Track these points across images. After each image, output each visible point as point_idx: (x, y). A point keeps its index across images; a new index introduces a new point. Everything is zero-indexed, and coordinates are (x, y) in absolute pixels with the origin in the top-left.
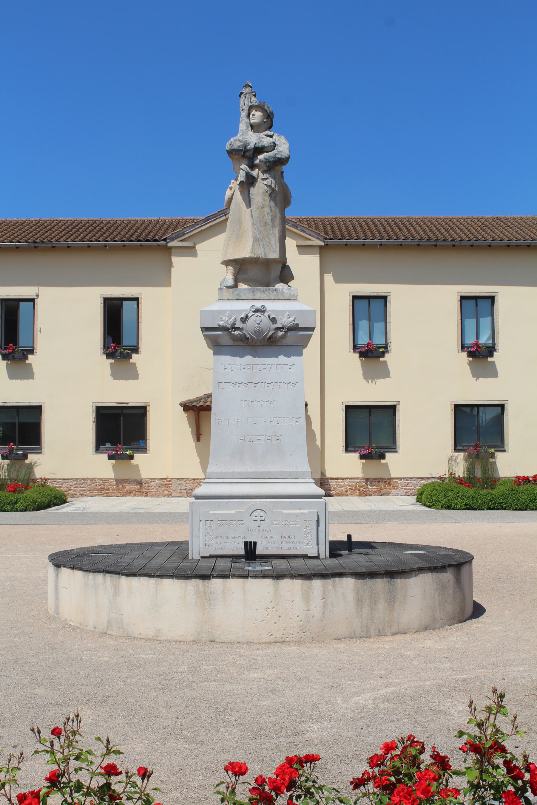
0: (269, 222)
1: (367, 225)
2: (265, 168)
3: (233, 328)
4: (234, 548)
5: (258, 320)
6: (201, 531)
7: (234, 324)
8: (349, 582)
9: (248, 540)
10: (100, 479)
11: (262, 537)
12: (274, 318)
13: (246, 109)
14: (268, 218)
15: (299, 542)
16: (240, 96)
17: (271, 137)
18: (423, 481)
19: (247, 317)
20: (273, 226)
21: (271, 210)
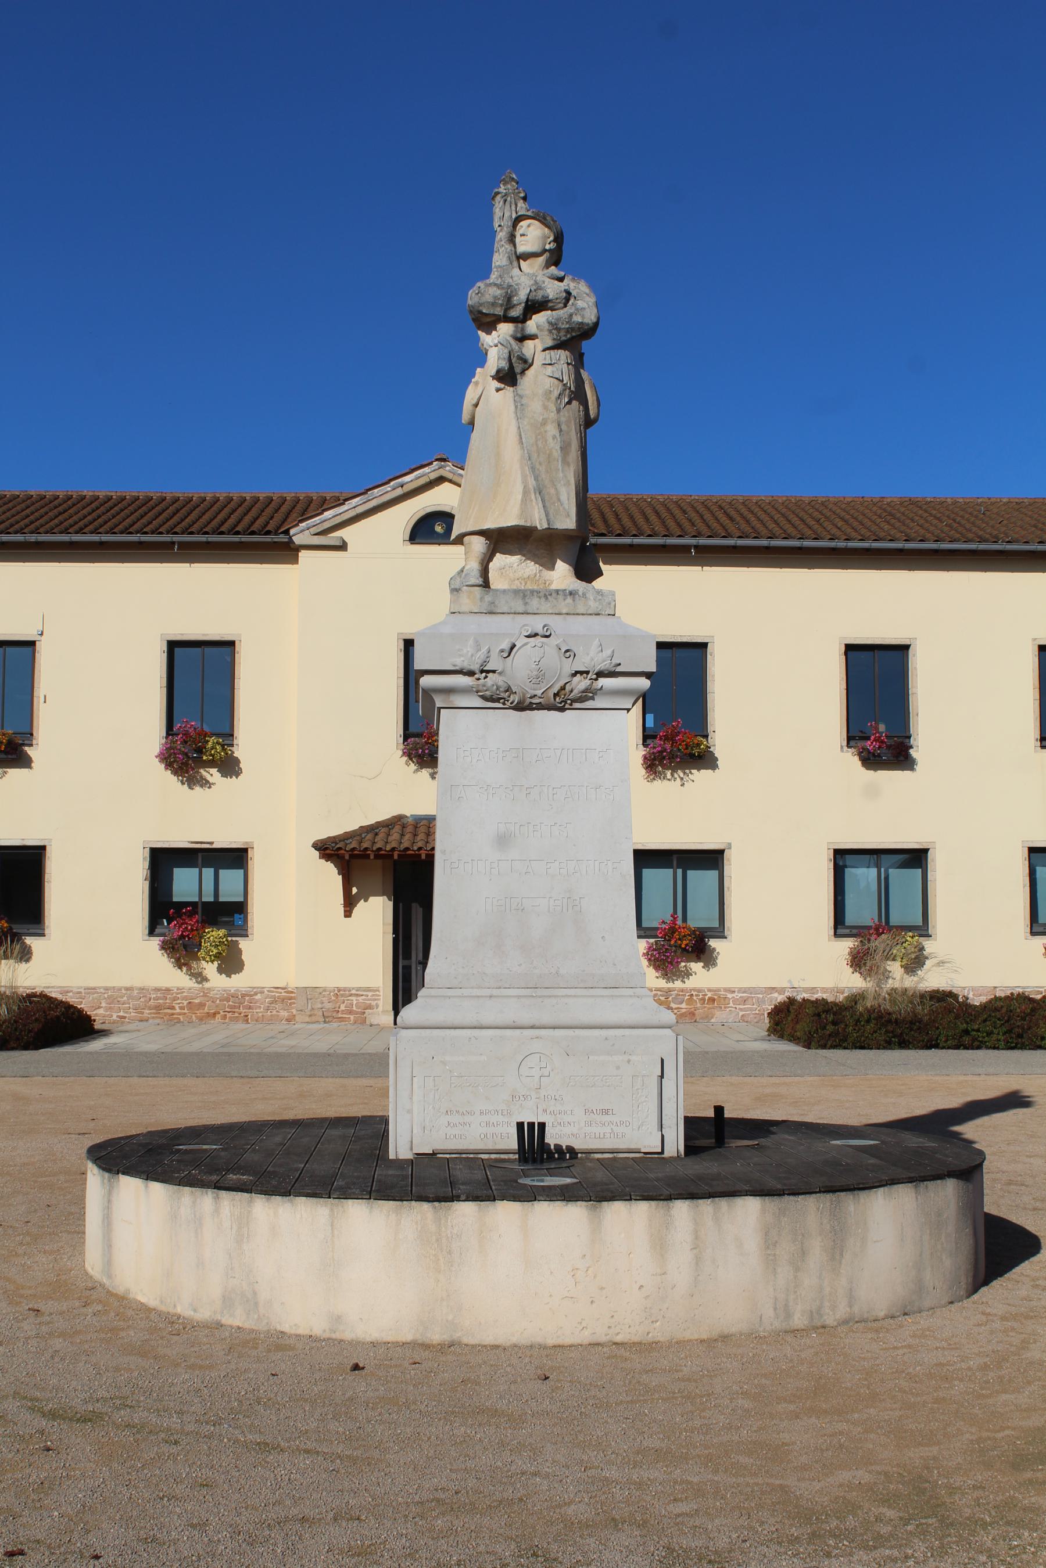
0: (557, 453)
1: (668, 510)
2: (550, 343)
3: (482, 671)
4: (486, 1136)
6: (415, 1098)
7: (486, 662)
8: (749, 1210)
9: (526, 1119)
10: (157, 990)
11: (545, 1111)
12: (567, 651)
13: (507, 223)
14: (554, 446)
15: (622, 1123)
16: (493, 198)
17: (561, 279)
18: (776, 995)
19: (513, 646)
20: (565, 462)
21: (561, 431)
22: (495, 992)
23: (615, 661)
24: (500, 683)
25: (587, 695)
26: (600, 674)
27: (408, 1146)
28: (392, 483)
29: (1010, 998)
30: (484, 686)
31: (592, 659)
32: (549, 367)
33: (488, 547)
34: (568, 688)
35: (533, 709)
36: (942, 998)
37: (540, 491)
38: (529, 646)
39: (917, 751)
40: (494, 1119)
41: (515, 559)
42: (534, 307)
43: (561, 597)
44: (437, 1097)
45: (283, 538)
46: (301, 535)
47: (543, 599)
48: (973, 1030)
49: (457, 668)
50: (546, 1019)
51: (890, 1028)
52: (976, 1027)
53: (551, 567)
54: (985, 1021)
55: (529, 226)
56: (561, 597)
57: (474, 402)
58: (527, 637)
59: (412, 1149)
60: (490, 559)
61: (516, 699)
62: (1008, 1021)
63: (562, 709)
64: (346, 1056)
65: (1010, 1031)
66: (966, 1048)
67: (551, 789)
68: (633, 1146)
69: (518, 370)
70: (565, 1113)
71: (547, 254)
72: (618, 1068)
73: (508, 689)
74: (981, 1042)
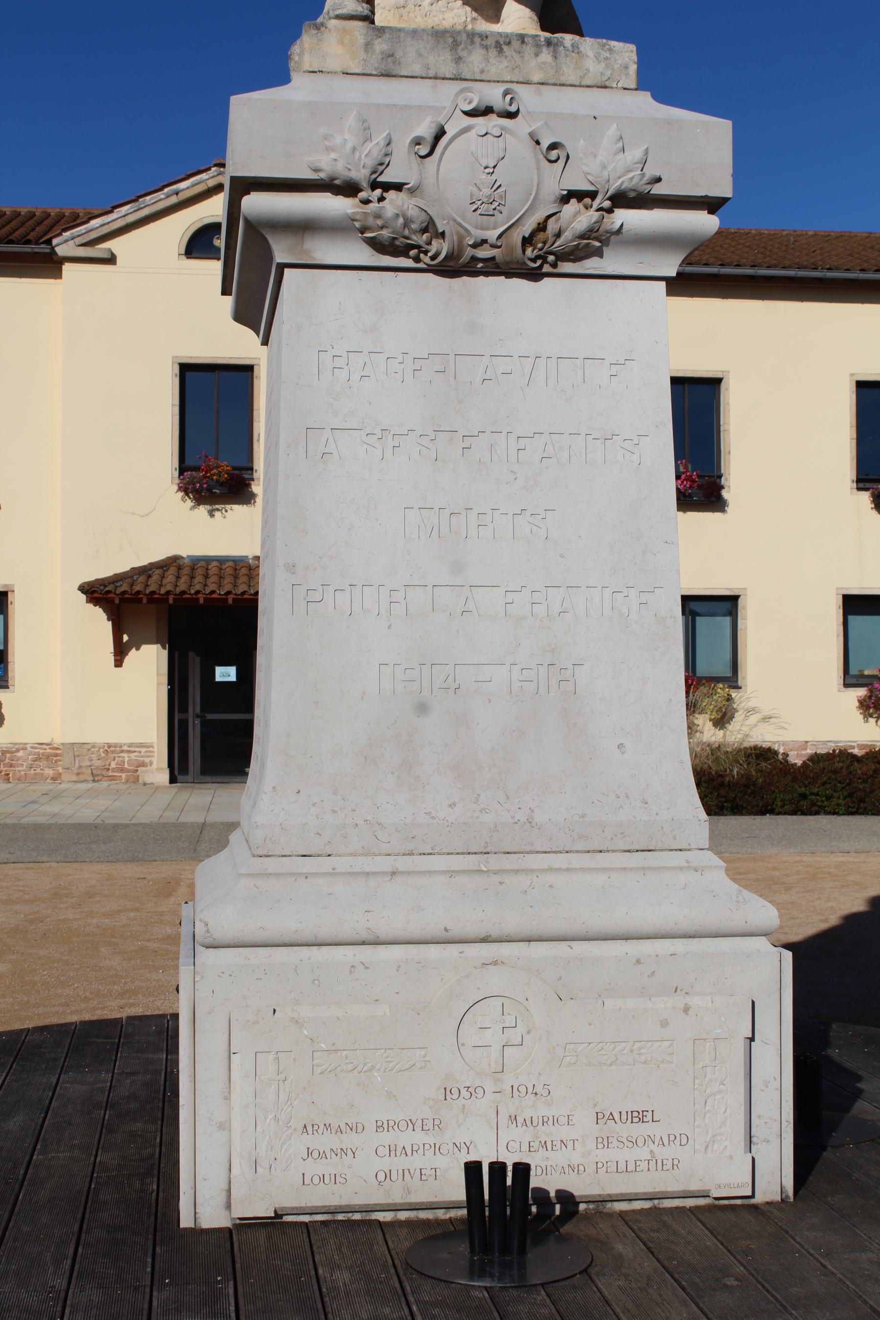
4: (388, 1175)
5: (488, 151)
6: (235, 1097)
7: (382, 165)
11: (513, 1119)
12: (553, 146)
15: (672, 1138)
19: (440, 133)
22: (404, 864)
23: (651, 171)
24: (412, 212)
25: (592, 243)
26: (622, 199)
27: (222, 1199)
28: (166, 190)
29: (830, 757)
30: (378, 216)
31: (604, 167)
34: (552, 227)
35: (475, 274)
36: (763, 755)
38: (472, 134)
39: (729, 492)
40: (406, 1138)
43: (529, 50)
44: (283, 1097)
45: (43, 248)
46: (64, 246)
47: (493, 53)
48: (812, 794)
49: (322, 175)
50: (513, 923)
51: (723, 792)
52: (816, 790)
54: (824, 784)
56: (529, 50)
58: (469, 114)
59: (228, 1206)
61: (441, 247)
62: (849, 784)
63: (535, 275)
64: (116, 827)
65: (850, 795)
66: (804, 813)
67: (512, 438)
68: (694, 1186)
70: (556, 1121)
72: (664, 1024)
73: (429, 227)
74: (820, 807)
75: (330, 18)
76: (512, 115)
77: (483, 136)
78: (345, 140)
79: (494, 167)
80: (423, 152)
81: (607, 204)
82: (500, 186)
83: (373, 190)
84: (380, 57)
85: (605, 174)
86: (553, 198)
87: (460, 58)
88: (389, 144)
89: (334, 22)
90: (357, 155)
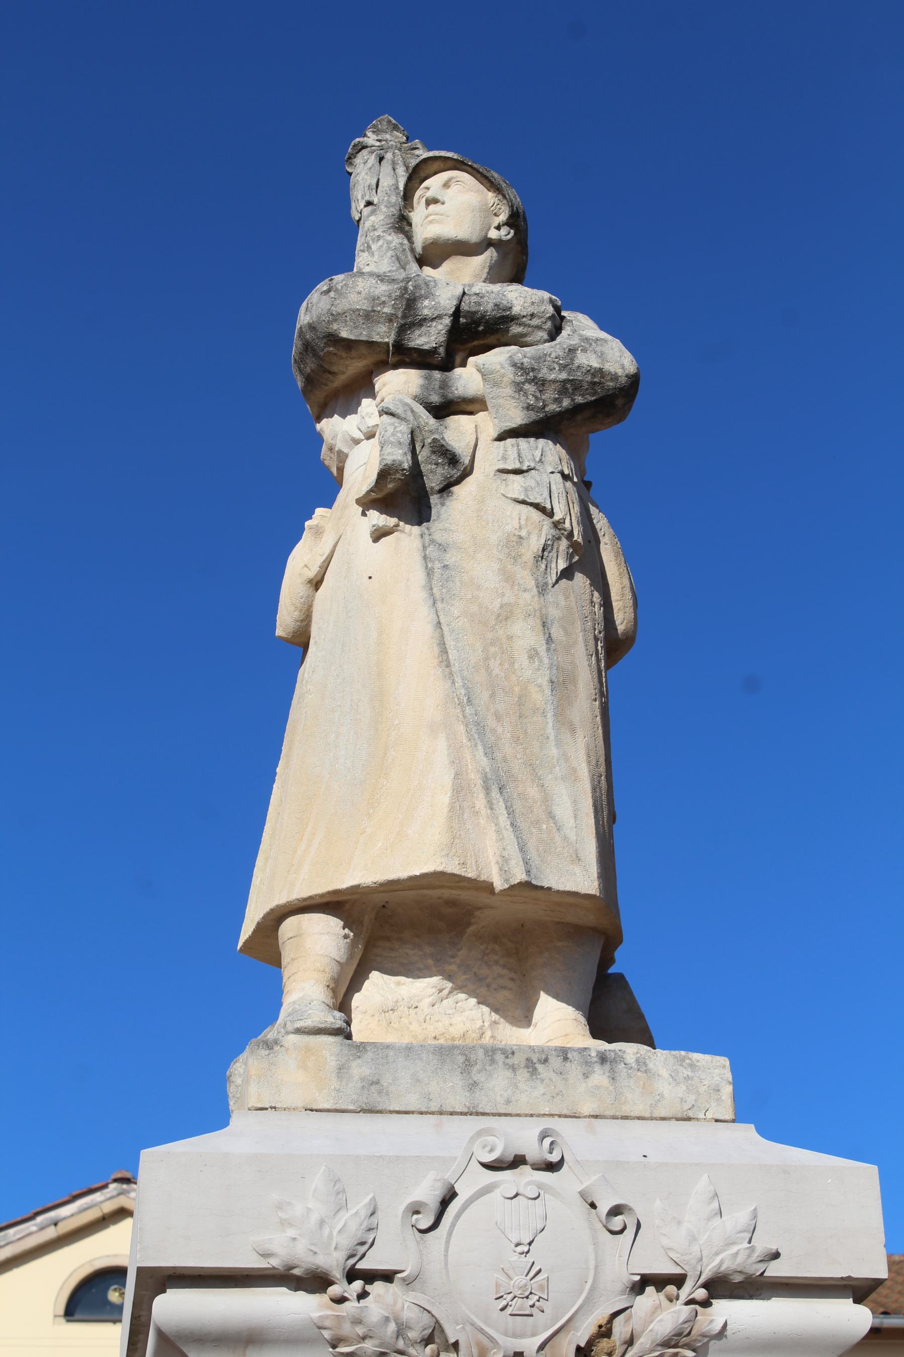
0: (541, 695)
3: (352, 1275)
5: (521, 1220)
7: (365, 1244)
12: (616, 1211)
14: (535, 678)
21: (549, 640)
23: (764, 1243)
24: (410, 1314)
28: (40, 1219)
30: (357, 1321)
31: (693, 1239)
32: (512, 488)
33: (351, 956)
34: (620, 1329)
37: (497, 783)
38: (497, 1195)
41: (422, 989)
42: (474, 332)
43: (574, 1069)
47: (523, 1074)
49: (274, 1262)
53: (525, 1018)
55: (446, 185)
56: (574, 1069)
57: (311, 573)
58: (488, 1166)
60: (356, 983)
69: (433, 481)
71: (490, 254)
75: (287, 1033)
76: (552, 1167)
77: (512, 1198)
78: (309, 1210)
79: (530, 1244)
80: (424, 1225)
81: (701, 1294)
82: (540, 1271)
83: (350, 1281)
84: (359, 1085)
85: (695, 1249)
86: (619, 1286)
87: (475, 1084)
88: (373, 1214)
89: (293, 1038)
90: (326, 1231)
